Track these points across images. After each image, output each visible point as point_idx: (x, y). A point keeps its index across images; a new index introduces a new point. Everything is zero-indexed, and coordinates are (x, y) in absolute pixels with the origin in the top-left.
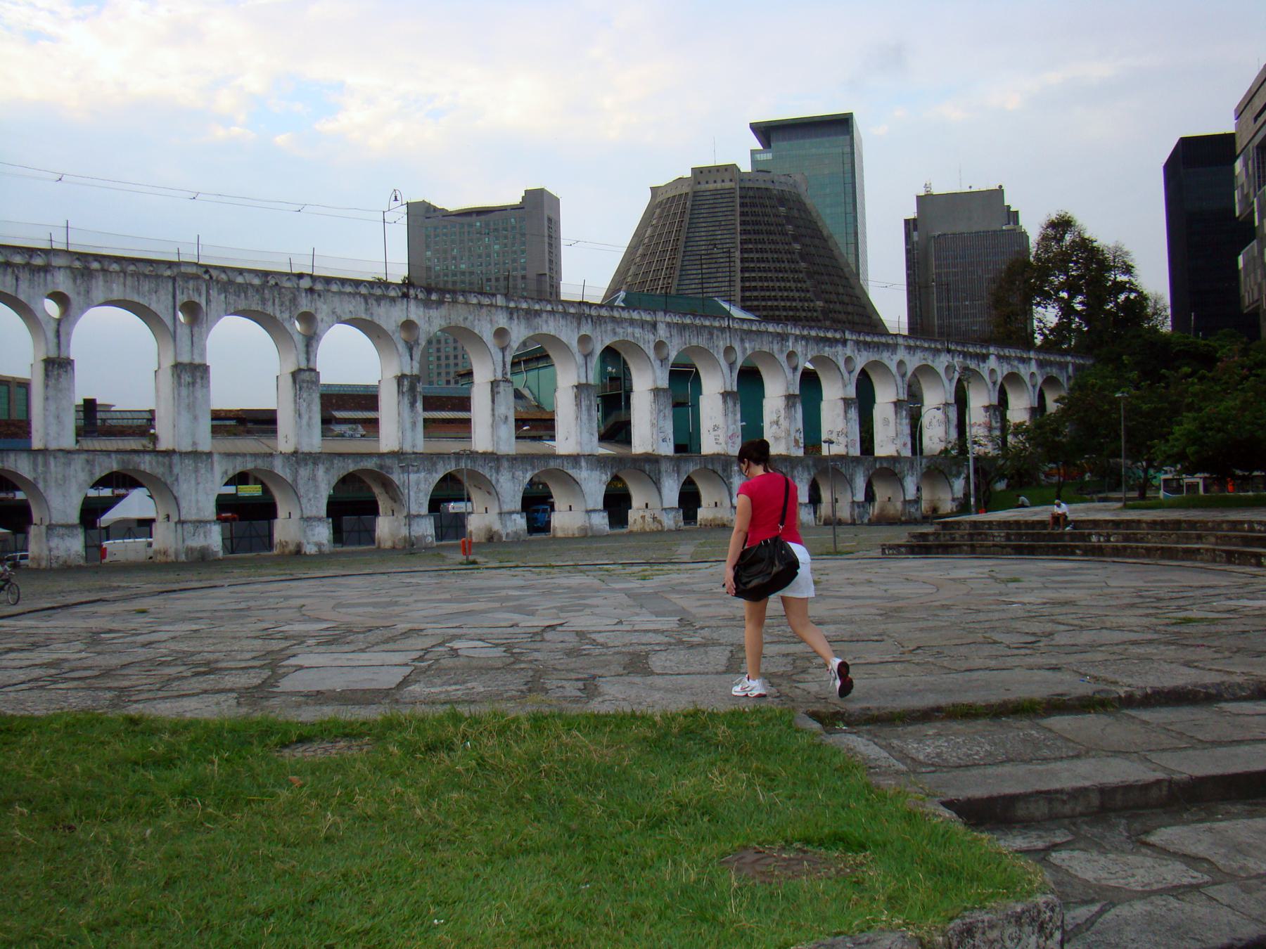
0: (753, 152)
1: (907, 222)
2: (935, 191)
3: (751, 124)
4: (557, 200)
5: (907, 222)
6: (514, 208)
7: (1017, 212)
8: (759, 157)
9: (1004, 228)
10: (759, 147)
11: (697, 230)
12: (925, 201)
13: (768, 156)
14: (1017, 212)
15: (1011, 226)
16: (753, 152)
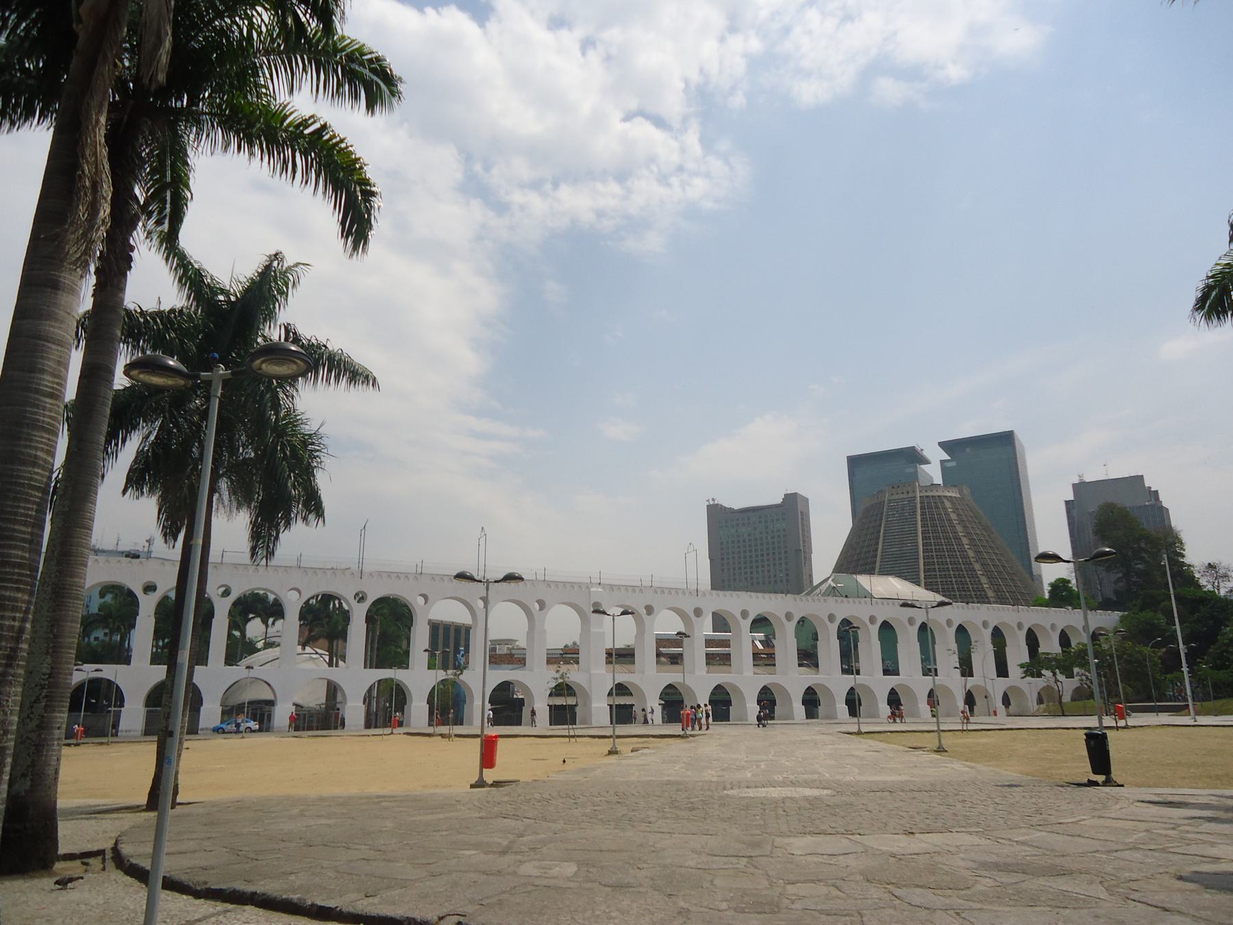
0: (942, 462)
1: (1067, 503)
2: (1088, 479)
3: (940, 444)
4: (808, 499)
5: (1067, 503)
6: (777, 506)
7: (1157, 491)
8: (950, 465)
9: (1147, 503)
10: (946, 457)
11: (892, 525)
12: (1079, 487)
13: (954, 464)
14: (1157, 491)
15: (1153, 502)
16: (942, 462)
